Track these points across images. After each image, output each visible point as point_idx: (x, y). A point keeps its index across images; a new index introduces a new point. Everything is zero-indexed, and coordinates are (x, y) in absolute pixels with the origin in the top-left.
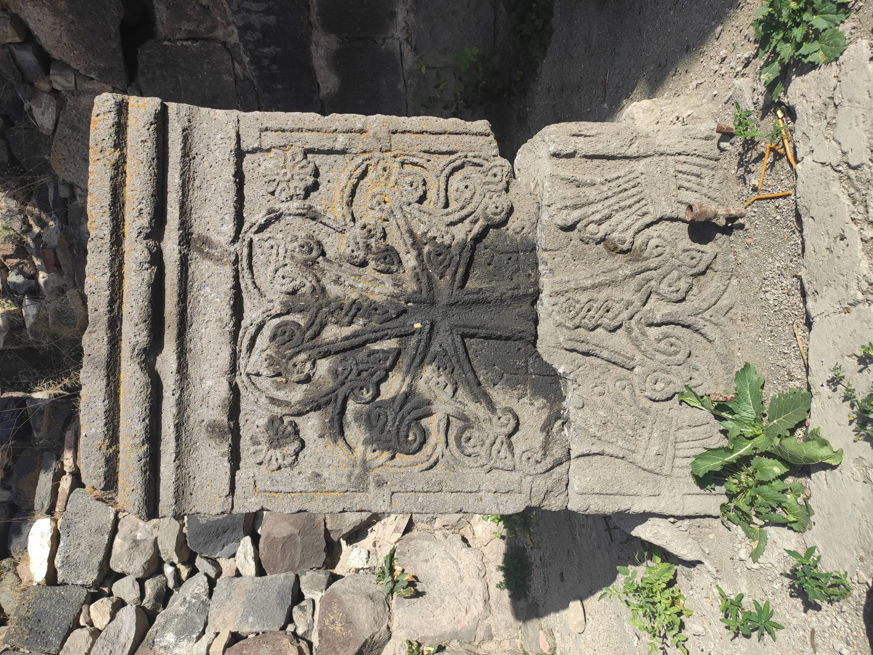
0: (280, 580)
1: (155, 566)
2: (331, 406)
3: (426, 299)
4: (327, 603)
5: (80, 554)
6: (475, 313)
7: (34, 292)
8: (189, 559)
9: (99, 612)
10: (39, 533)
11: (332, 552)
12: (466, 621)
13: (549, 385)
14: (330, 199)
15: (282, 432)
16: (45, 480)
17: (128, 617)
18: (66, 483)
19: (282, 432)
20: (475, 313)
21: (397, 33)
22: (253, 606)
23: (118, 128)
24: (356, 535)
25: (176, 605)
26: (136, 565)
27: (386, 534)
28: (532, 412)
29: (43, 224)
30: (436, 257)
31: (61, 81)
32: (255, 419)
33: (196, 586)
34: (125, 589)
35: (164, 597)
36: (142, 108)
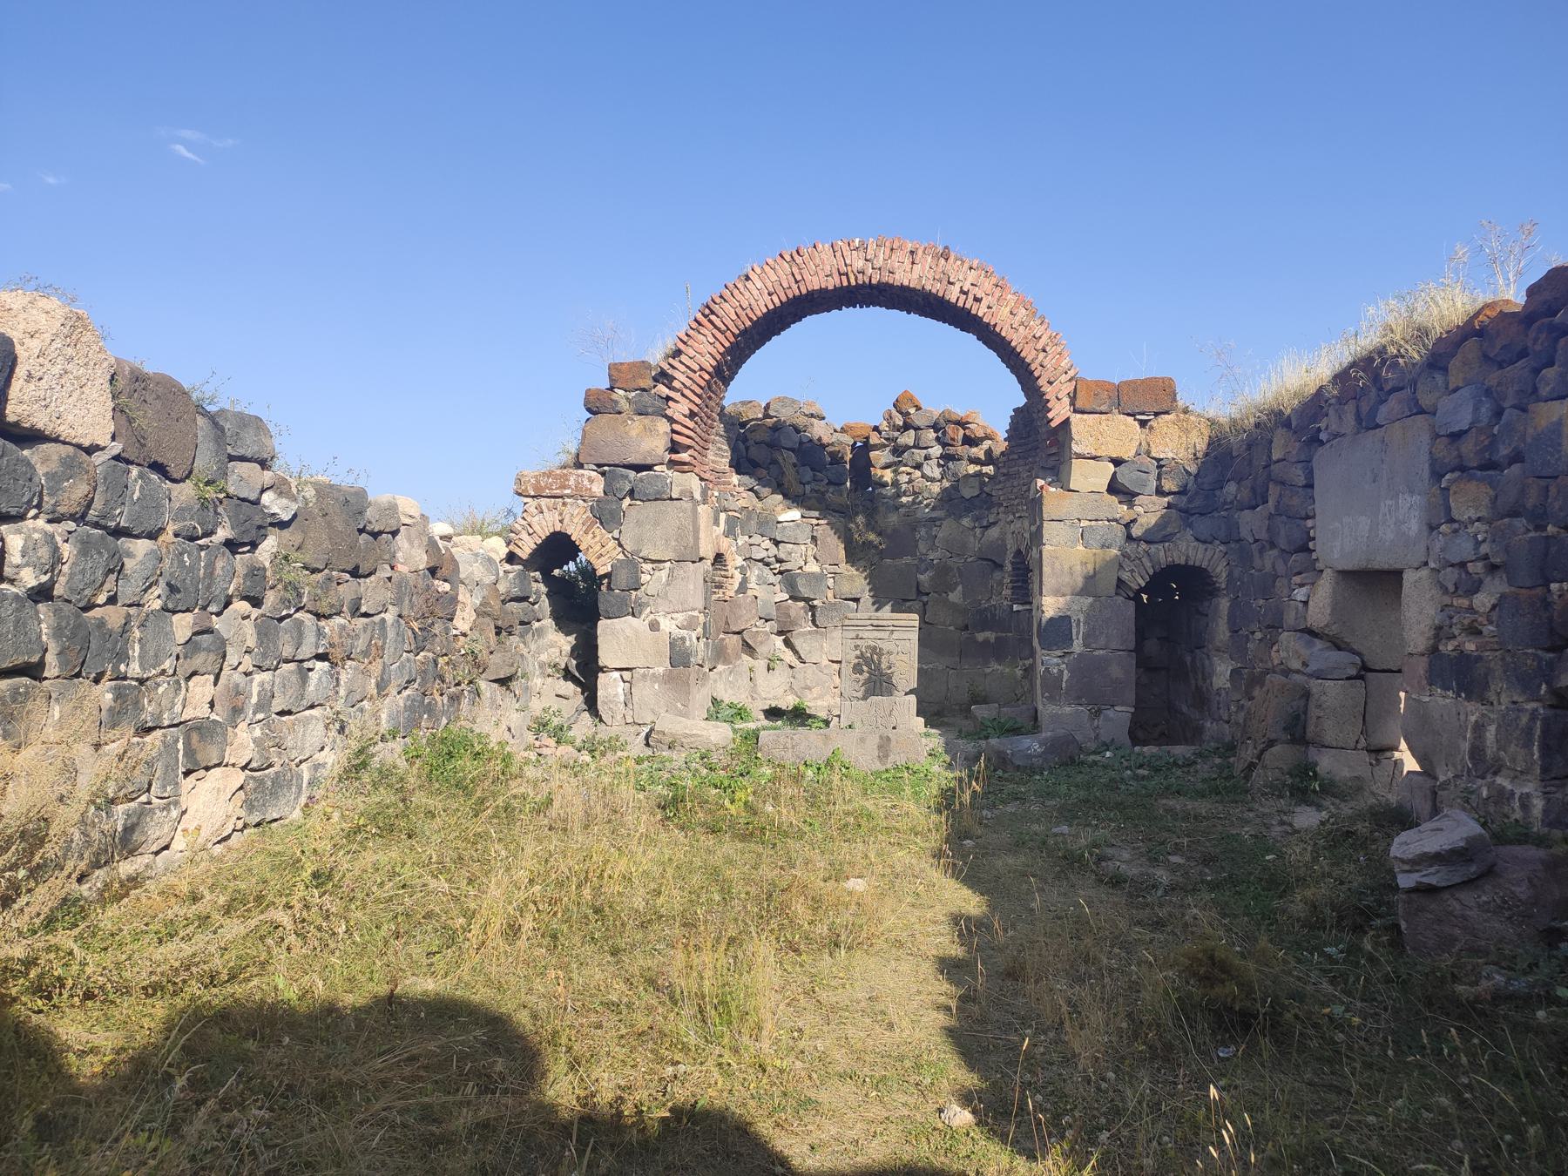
0: (774, 614)
1: (780, 561)
2: (862, 656)
3: (882, 674)
4: (765, 633)
5: (788, 533)
6: (877, 682)
7: (899, 496)
8: (781, 573)
9: (767, 544)
10: (795, 514)
11: (780, 633)
12: (760, 690)
13: (865, 698)
14: (901, 657)
15: (857, 647)
16: (816, 514)
17: (762, 554)
18: (814, 522)
19: (857, 647)
20: (877, 682)
21: (996, 666)
22: (765, 603)
23: (913, 619)
24: (788, 643)
25: (766, 570)
26: (782, 556)
27: (789, 656)
28: (860, 694)
29: (927, 506)
30: (890, 677)
31: (978, 531)
32: (859, 642)
33: (772, 579)
34: (773, 550)
35: (767, 564)
36: (917, 624)
